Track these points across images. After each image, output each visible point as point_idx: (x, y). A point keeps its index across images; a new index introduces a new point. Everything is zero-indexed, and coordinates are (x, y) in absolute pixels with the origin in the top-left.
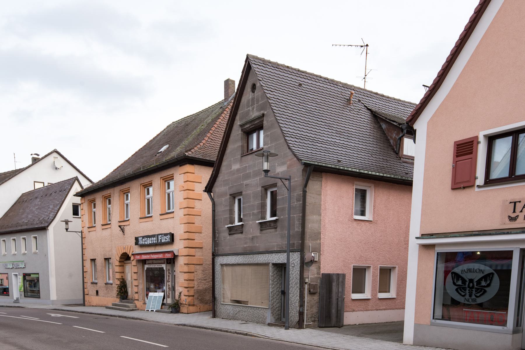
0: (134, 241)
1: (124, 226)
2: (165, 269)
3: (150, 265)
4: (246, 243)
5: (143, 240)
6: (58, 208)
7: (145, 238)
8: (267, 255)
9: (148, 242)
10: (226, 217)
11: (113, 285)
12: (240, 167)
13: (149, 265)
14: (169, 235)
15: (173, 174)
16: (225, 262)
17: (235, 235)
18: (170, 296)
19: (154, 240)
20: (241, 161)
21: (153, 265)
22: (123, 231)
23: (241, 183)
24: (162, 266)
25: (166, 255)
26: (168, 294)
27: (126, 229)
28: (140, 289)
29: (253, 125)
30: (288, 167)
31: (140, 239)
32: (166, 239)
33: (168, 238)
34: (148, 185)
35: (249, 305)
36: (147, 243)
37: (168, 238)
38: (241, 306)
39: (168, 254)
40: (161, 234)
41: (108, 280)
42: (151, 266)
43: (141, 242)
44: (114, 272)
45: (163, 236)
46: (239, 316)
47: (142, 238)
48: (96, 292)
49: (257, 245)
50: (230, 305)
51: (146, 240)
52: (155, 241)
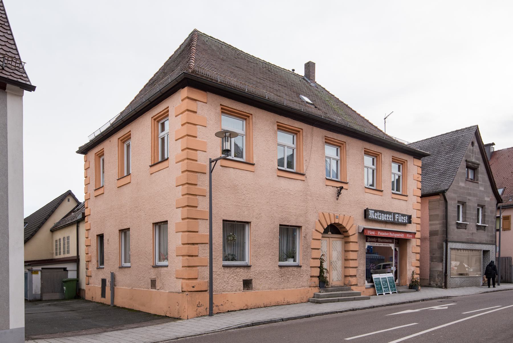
2: (393, 248)
3: (374, 243)
4: (468, 236)
5: (376, 214)
7: (378, 213)
8: (480, 245)
9: (382, 218)
10: (455, 216)
12: (464, 186)
13: (372, 243)
14: (407, 216)
16: (453, 247)
17: (461, 230)
19: (390, 218)
20: (465, 183)
21: (378, 243)
23: (466, 196)
24: (390, 246)
25: (407, 236)
28: (360, 271)
29: (473, 166)
30: (490, 200)
31: (371, 212)
32: (403, 220)
33: (405, 219)
34: (370, 154)
35: (470, 276)
36: (380, 219)
37: (405, 219)
38: (466, 277)
39: (410, 235)
40: (398, 214)
41: (123, 263)
42: (374, 244)
44: (309, 250)
45: (400, 216)
46: (464, 284)
48: (242, 283)
49: (475, 238)
50: (458, 277)
51: (379, 215)
52: (391, 218)
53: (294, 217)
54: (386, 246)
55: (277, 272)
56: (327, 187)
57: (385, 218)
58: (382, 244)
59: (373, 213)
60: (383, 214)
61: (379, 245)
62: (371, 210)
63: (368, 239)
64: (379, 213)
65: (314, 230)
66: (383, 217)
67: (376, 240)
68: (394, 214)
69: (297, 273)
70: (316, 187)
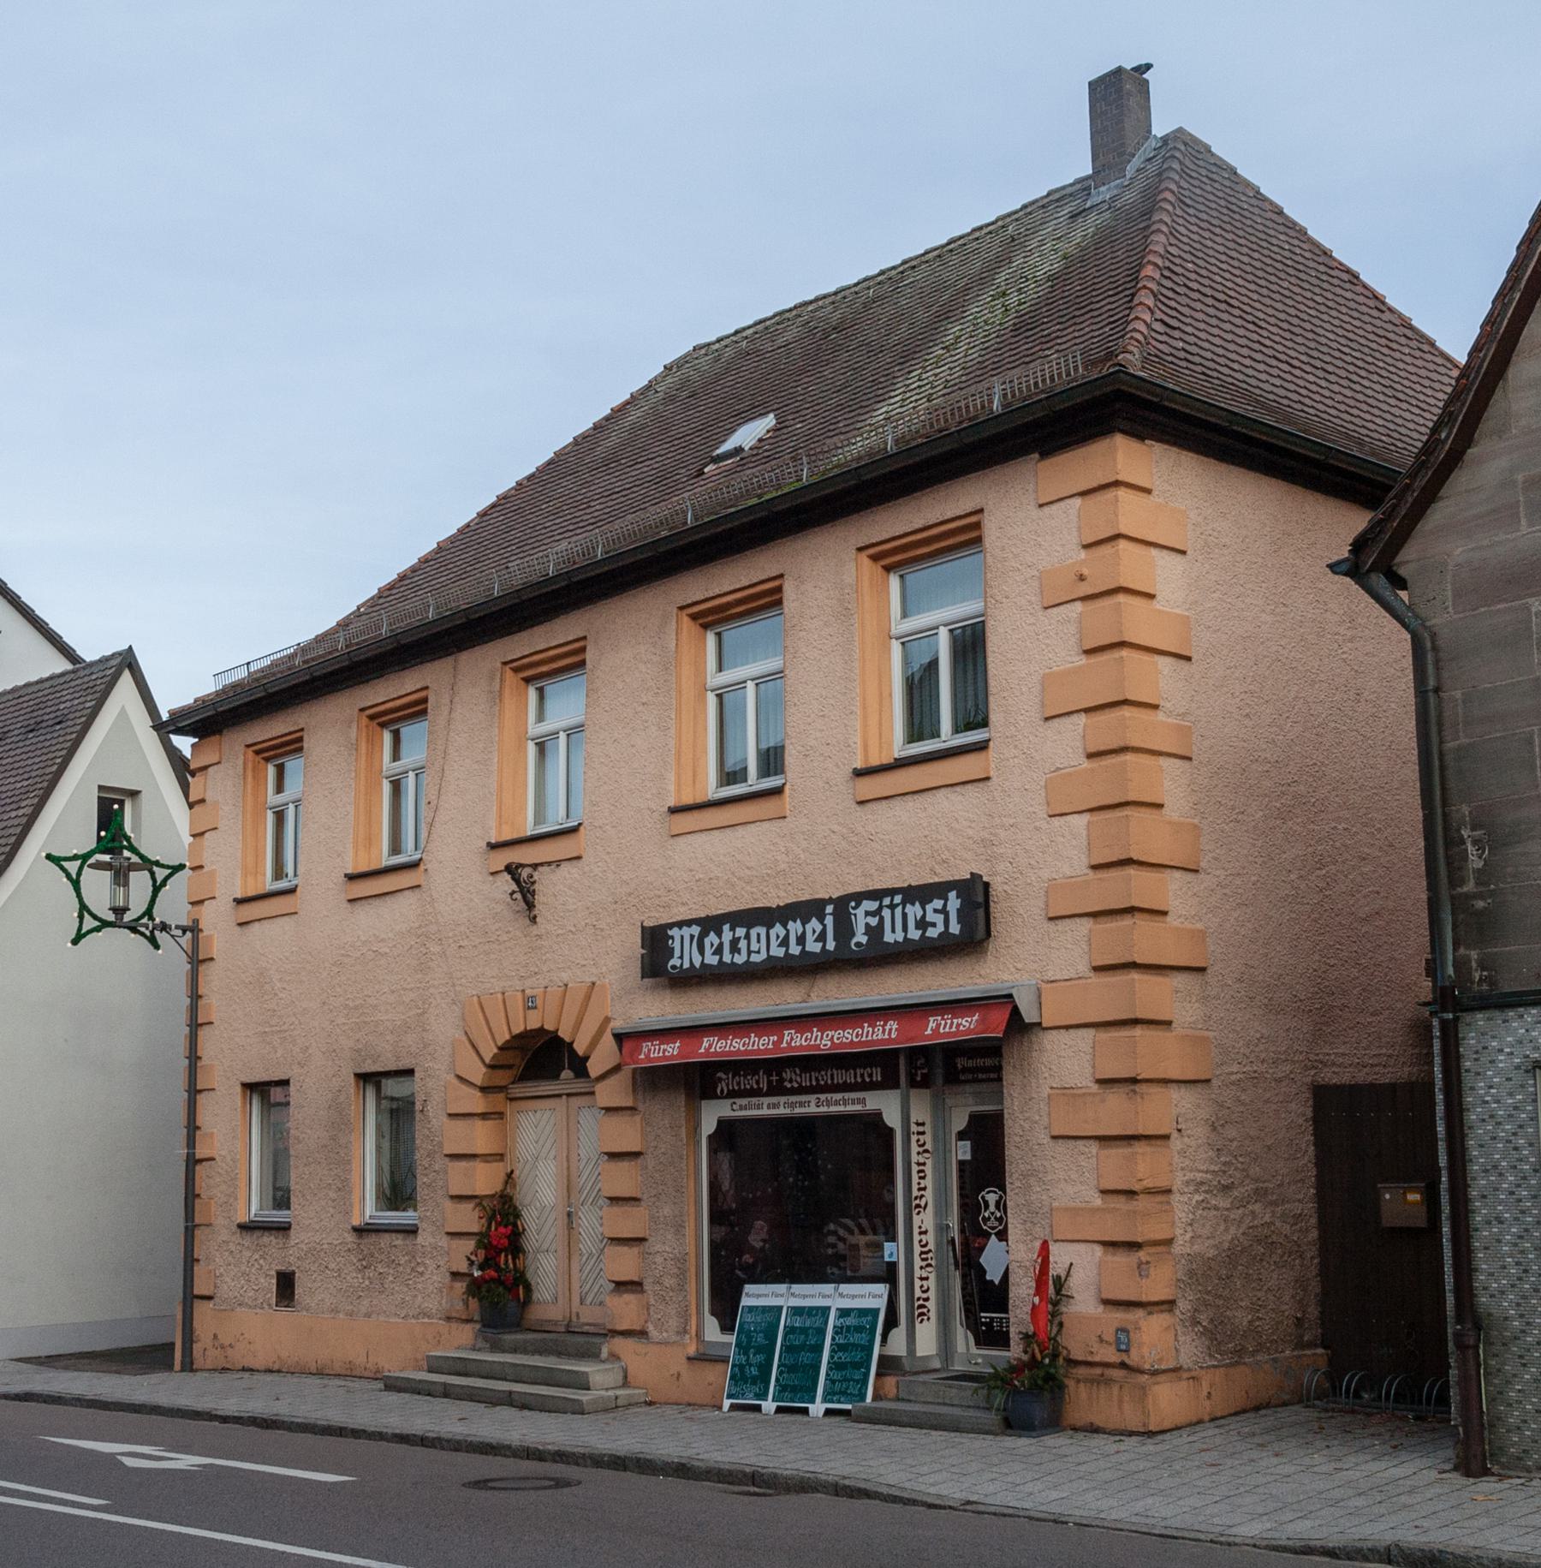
0: (634, 945)
1: (535, 866)
2: (892, 1119)
3: (754, 1100)
5: (712, 938)
6: (28, 811)
7: (726, 927)
9: (749, 952)
11: (419, 1239)
13: (744, 1101)
15: (981, 511)
18: (931, 1305)
19: (814, 937)
21: (783, 1099)
22: (526, 894)
26: (918, 1293)
27: (549, 885)
28: (659, 1259)
33: (944, 911)
37: (944, 911)
42: (759, 1107)
43: (685, 953)
45: (892, 907)
47: (696, 930)
52: (822, 937)
53: (388, 1038)
54: (841, 1108)
55: (349, 1250)
56: (495, 882)
57: (774, 943)
58: (812, 1098)
59: (692, 937)
60: (762, 924)
61: (792, 1105)
62: (680, 924)
63: (720, 1079)
64: (732, 929)
65: (451, 1078)
66: (762, 945)
67: (770, 1082)
68: (843, 905)
69: (407, 1258)
70: (457, 897)
